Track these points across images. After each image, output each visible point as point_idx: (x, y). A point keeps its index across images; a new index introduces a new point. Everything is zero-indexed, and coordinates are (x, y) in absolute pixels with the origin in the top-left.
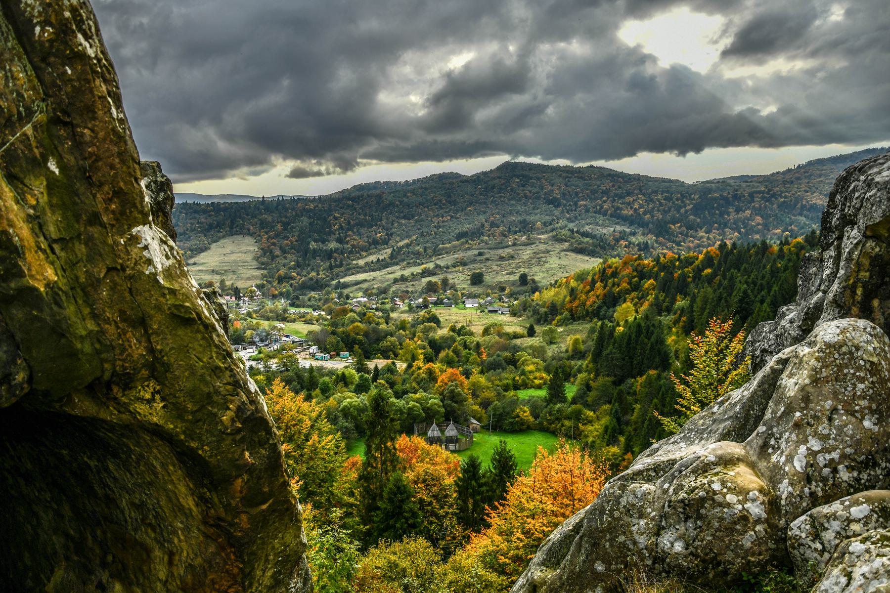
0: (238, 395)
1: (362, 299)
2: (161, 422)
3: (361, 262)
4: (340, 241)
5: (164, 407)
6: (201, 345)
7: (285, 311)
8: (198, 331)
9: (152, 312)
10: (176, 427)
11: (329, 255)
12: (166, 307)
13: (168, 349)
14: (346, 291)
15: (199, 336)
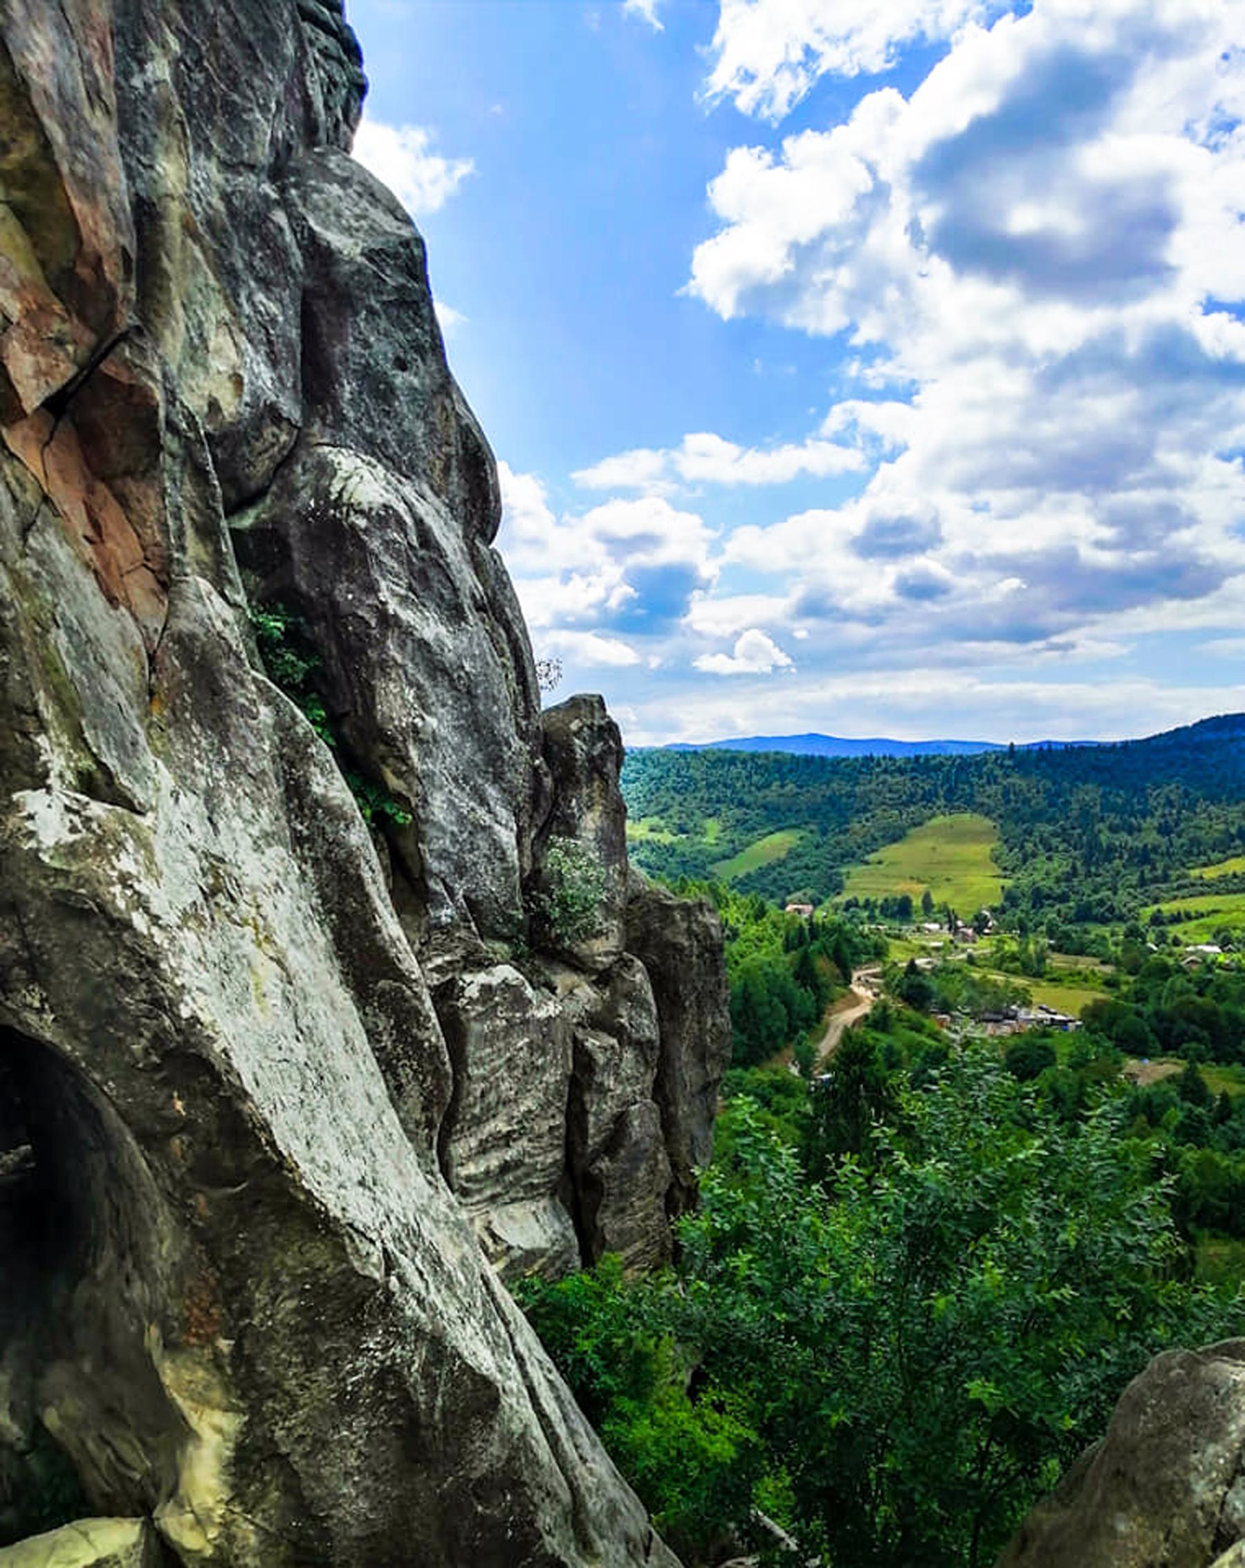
0: (157, 1017)
1: (1207, 949)
2: (56, 1040)
3: (1210, 873)
4: (1164, 830)
5: (54, 1020)
6: (101, 946)
7: (1041, 959)
8: (99, 927)
9: (28, 897)
10: (74, 1049)
11: (1143, 857)
12: (47, 893)
13: (49, 945)
14: (1174, 931)
15: (100, 934)
